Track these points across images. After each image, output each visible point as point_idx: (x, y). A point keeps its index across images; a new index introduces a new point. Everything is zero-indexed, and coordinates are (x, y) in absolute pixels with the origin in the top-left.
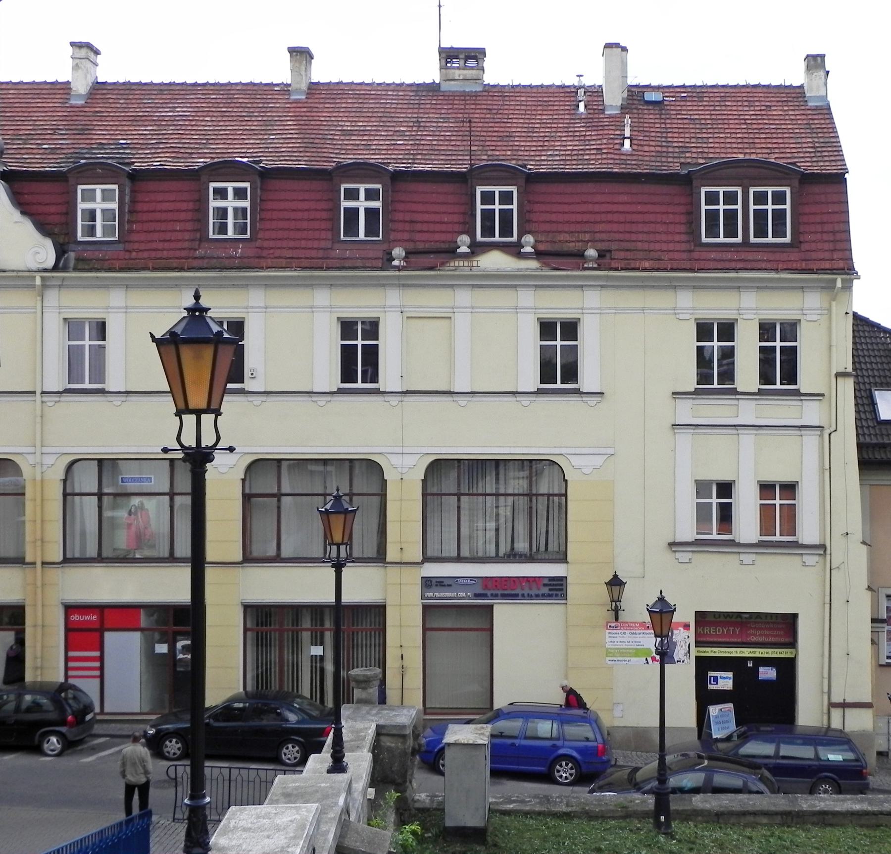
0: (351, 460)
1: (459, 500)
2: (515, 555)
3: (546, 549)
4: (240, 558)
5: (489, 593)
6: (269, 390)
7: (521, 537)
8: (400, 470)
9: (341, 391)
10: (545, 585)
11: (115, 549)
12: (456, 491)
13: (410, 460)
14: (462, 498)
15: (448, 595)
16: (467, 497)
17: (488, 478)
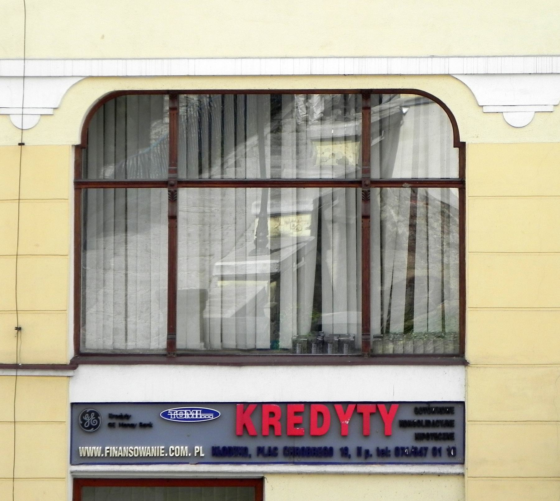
1: (173, 198)
2: (323, 345)
3: (409, 329)
5: (252, 445)
7: (341, 297)
8: (16, 120)
10: (404, 424)
12: (164, 175)
14: (183, 193)
15: (143, 450)
16: (195, 191)
17: (253, 141)
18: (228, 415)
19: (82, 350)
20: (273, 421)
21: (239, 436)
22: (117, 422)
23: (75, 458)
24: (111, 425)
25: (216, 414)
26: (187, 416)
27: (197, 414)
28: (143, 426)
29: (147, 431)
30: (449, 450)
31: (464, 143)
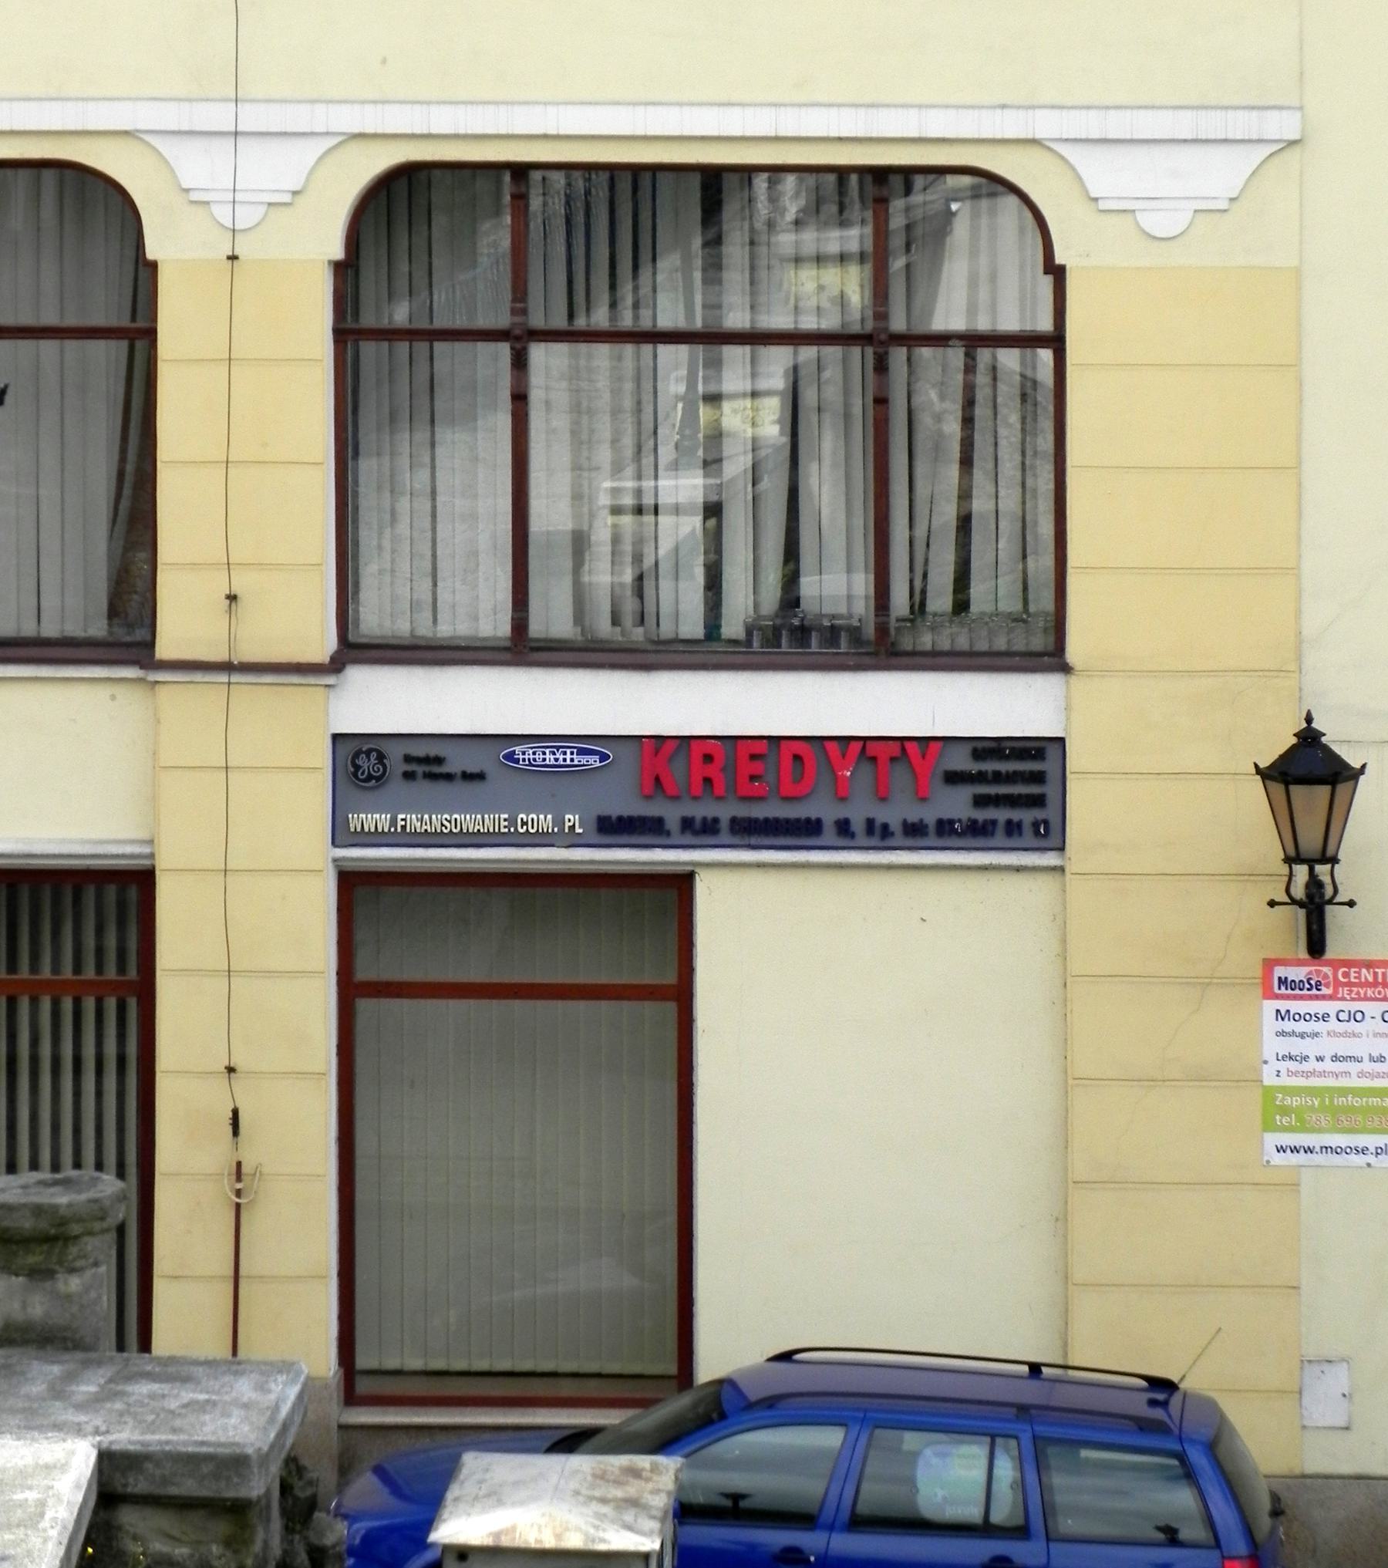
5: (673, 814)
10: (954, 778)
15: (470, 822)
18: (629, 759)
20: (710, 771)
21: (648, 797)
22: (420, 769)
23: (341, 834)
24: (409, 776)
25: (604, 757)
26: (550, 759)
28: (467, 777)
30: (1036, 825)
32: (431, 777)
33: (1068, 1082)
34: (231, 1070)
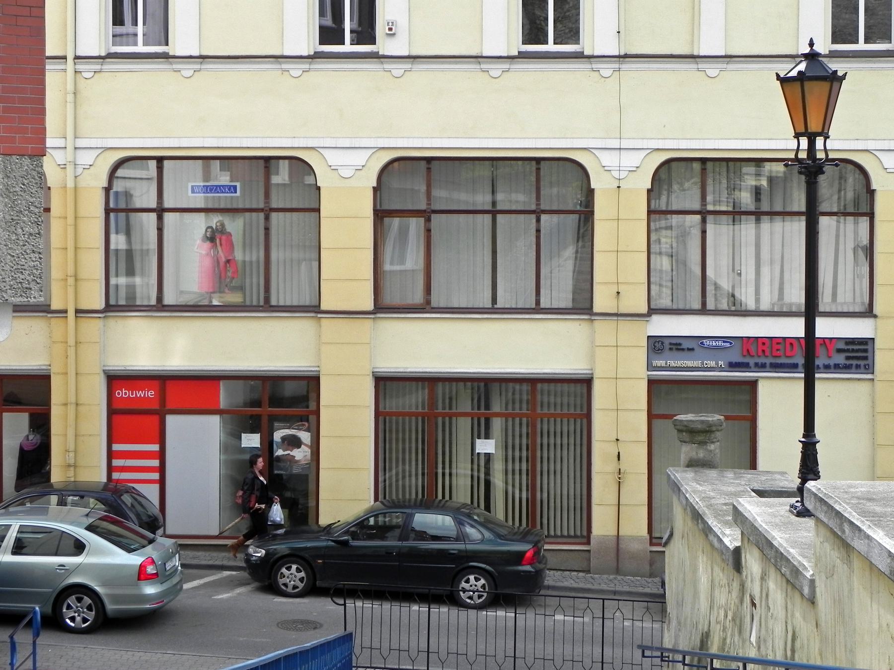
0: (538, 160)
4: (369, 306)
5: (752, 362)
6: (414, 53)
9: (523, 56)
10: (839, 351)
11: (182, 292)
13: (631, 160)
15: (690, 363)
18: (738, 345)
19: (652, 307)
20: (764, 348)
21: (744, 356)
22: (674, 347)
23: (650, 367)
24: (671, 349)
25: (731, 343)
26: (714, 344)
27: (720, 343)
28: (689, 349)
29: (690, 353)
30: (865, 366)
31: (874, 190)
32: (678, 349)
33: (874, 445)
34: (617, 440)
